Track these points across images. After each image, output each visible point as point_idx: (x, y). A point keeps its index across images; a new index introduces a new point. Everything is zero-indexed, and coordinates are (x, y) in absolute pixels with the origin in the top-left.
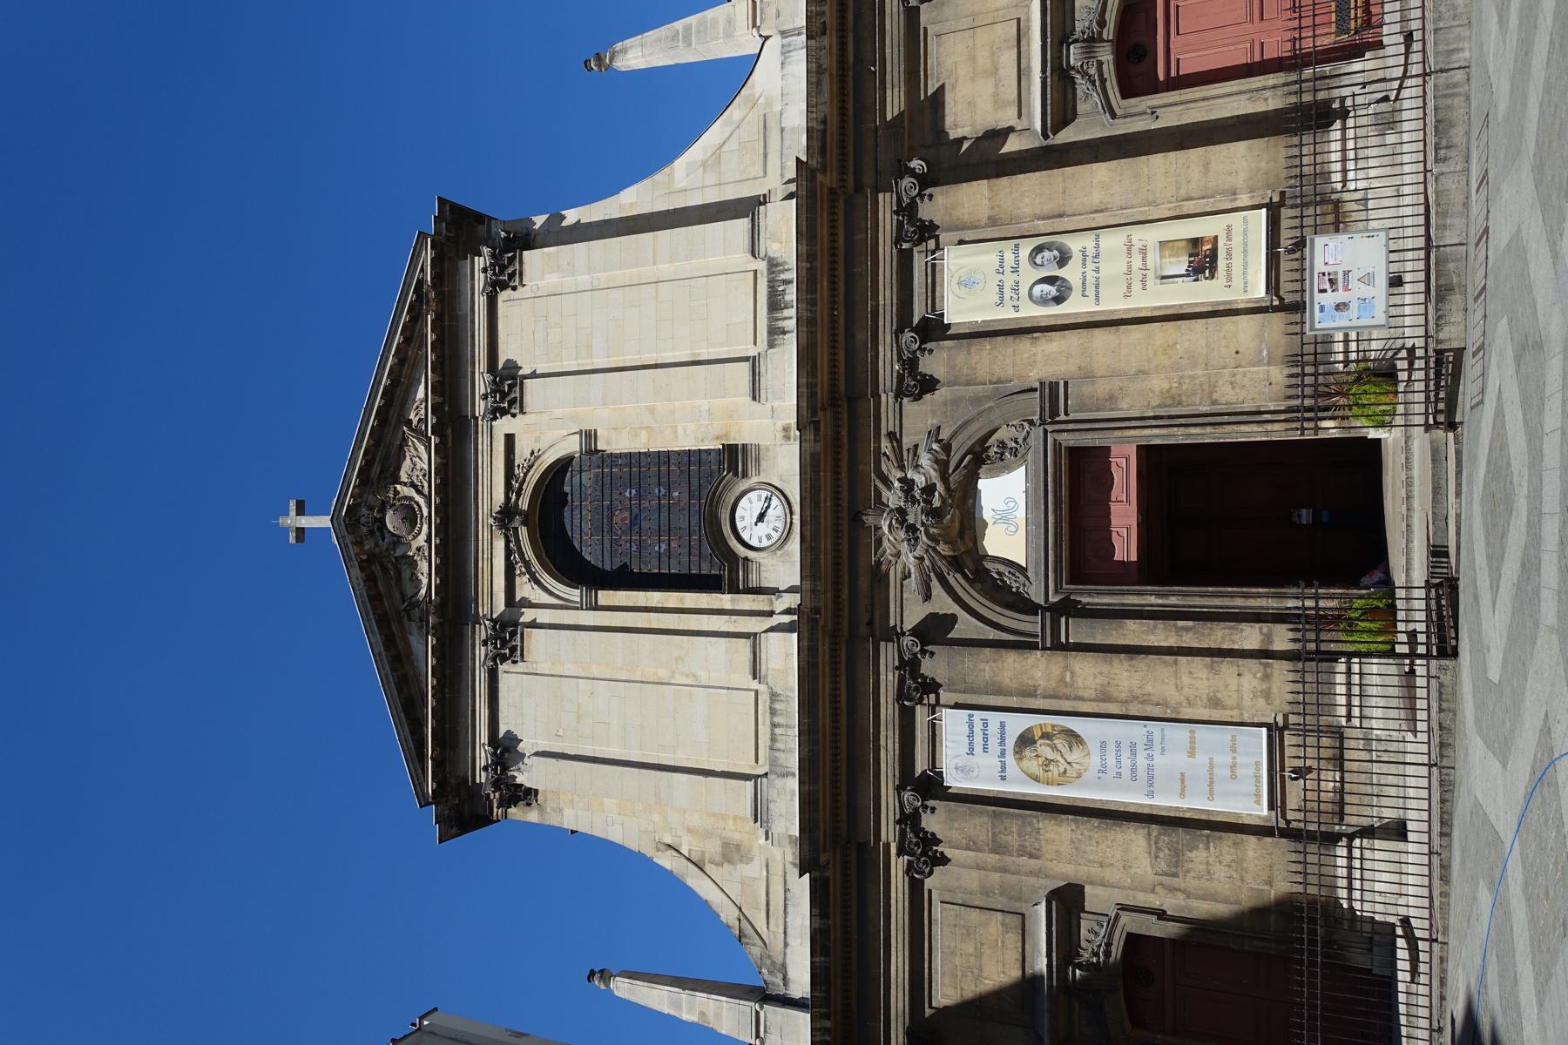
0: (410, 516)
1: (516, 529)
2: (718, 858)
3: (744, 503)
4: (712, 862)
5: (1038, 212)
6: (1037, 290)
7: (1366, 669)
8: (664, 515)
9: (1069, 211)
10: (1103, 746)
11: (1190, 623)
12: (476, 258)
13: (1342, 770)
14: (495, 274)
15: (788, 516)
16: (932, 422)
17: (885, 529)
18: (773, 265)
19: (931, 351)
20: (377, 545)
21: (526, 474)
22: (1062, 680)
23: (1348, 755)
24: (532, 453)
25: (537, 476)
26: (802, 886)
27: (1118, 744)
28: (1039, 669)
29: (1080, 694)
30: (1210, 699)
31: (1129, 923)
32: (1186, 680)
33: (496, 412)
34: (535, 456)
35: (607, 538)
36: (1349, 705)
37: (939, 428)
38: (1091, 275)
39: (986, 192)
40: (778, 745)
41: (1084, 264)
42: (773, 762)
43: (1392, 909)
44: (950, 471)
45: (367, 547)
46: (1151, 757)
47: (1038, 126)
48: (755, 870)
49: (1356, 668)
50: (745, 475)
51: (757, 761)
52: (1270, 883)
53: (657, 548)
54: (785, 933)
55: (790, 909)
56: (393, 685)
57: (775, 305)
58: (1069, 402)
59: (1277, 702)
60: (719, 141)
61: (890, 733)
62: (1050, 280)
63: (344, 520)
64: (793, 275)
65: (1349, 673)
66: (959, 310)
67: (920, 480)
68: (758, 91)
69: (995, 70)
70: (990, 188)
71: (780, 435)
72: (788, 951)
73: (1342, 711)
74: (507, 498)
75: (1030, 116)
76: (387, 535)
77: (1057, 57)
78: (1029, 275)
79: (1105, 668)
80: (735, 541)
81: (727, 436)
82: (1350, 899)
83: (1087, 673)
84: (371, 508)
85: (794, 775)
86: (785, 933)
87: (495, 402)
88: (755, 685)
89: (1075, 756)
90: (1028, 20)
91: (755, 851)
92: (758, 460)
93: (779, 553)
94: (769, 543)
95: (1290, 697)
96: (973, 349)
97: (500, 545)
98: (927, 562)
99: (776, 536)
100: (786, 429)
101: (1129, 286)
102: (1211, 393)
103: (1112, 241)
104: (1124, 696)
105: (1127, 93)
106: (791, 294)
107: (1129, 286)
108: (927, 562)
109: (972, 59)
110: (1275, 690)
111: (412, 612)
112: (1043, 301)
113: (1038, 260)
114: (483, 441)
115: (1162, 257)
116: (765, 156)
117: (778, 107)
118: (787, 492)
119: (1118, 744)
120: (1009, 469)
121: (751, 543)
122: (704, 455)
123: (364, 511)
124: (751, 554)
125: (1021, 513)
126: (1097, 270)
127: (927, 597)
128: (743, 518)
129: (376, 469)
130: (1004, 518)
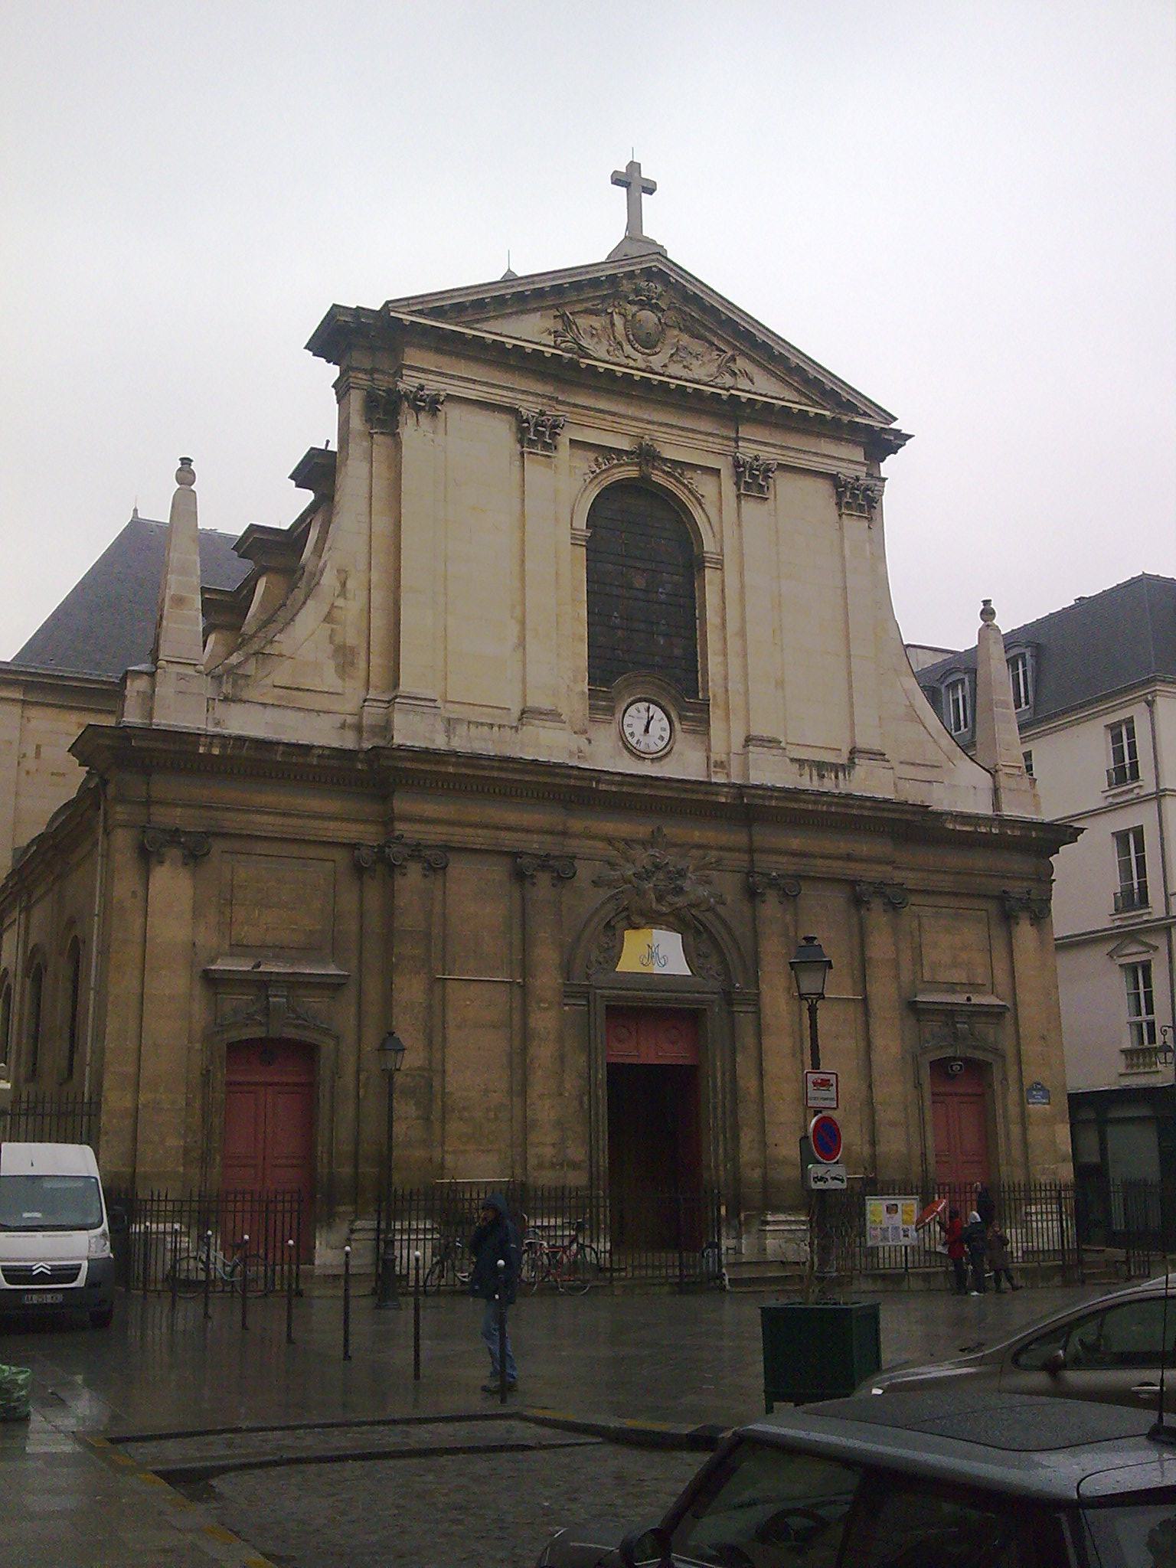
2: (338, 639)
3: (658, 714)
8: (642, 626)
9: (872, 1021)
14: (853, 488)
15: (651, 756)
16: (729, 899)
18: (848, 767)
31: (327, 1045)
37: (724, 904)
44: (693, 911)
48: (330, 679)
50: (681, 718)
51: (447, 702)
53: (615, 614)
56: (502, 292)
57: (821, 767)
58: (742, 1015)
63: (655, 266)
67: (687, 885)
75: (923, 991)
76: (635, 308)
80: (629, 701)
88: (516, 712)
92: (694, 732)
93: (620, 744)
94: (627, 735)
97: (625, 444)
99: (633, 741)
100: (721, 765)
106: (828, 785)
118: (667, 760)
124: (618, 715)
125: (657, 970)
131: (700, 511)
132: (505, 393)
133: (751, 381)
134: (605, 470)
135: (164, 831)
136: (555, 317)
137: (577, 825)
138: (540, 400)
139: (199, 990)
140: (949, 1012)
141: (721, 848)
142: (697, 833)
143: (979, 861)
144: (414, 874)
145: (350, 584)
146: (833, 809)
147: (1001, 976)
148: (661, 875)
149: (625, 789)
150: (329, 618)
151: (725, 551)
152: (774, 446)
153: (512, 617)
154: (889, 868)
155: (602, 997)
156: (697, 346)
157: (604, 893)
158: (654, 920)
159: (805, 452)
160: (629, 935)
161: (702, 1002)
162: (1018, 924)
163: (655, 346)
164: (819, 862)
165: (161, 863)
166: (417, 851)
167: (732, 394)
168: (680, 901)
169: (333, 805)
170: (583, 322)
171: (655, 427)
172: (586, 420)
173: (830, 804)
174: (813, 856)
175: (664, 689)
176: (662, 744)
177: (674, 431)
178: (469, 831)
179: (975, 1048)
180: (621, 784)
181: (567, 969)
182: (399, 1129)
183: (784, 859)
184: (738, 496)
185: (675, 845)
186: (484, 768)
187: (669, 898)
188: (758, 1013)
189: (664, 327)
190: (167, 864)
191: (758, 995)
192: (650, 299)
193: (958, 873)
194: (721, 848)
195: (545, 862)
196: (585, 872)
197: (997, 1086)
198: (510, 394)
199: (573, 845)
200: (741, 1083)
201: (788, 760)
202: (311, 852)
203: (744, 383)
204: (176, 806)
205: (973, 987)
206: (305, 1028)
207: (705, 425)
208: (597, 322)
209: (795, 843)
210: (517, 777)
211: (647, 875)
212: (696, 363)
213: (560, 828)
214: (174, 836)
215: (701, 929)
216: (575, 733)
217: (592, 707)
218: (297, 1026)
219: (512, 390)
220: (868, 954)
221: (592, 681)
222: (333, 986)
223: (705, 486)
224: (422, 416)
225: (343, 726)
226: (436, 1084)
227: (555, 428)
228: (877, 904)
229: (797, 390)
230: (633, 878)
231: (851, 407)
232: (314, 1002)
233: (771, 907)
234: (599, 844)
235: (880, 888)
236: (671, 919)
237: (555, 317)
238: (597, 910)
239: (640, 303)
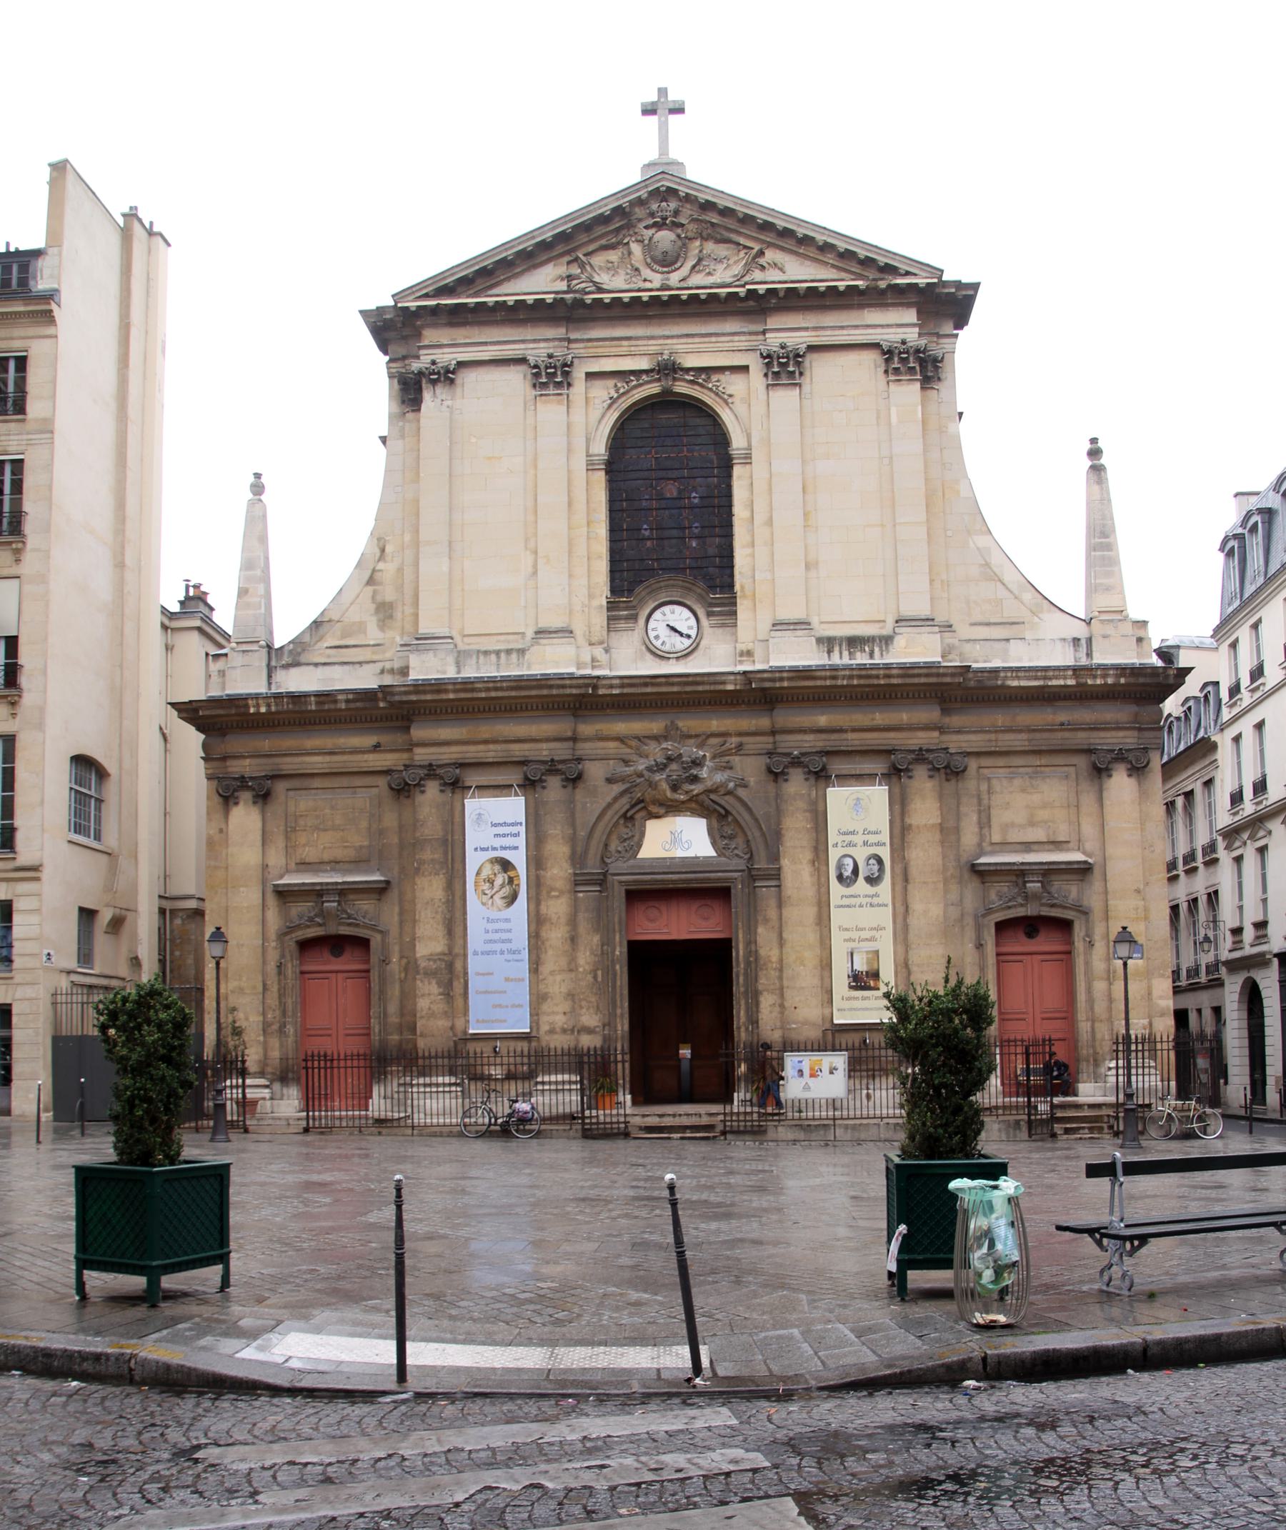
0: (667, 262)
1: (659, 380)
2: (379, 598)
3: (687, 613)
4: (375, 592)
5: (912, 863)
6: (849, 862)
7: (574, 1093)
9: (910, 887)
10: (507, 920)
11: (600, 979)
12: (917, 330)
13: (502, 1080)
14: (900, 353)
16: (752, 781)
17: (664, 745)
19: (807, 779)
20: (640, 220)
21: (710, 390)
22: (552, 889)
23: (513, 1083)
24: (730, 396)
25: (709, 401)
26: (366, 680)
27: (510, 931)
28: (559, 871)
29: (543, 903)
30: (546, 994)
31: (376, 940)
32: (559, 978)
33: (768, 358)
34: (726, 400)
35: (654, 475)
36: (550, 1083)
37: (745, 786)
38: (857, 901)
39: (931, 822)
40: (482, 657)
41: (866, 896)
42: (467, 654)
43: (416, 1110)
44: (713, 796)
45: (637, 210)
46: (502, 953)
47: (982, 860)
48: (374, 634)
49: (574, 1087)
50: (709, 614)
52: (421, 1035)
54: (325, 664)
55: (346, 668)
57: (854, 643)
59: (547, 1038)
60: (1006, 579)
61: (500, 754)
62: (856, 871)
64: (877, 660)
65: (570, 1082)
66: (838, 798)
67: (704, 773)
68: (1045, 616)
69: (1032, 823)
70: (933, 826)
71: (741, 647)
72: (311, 668)
73: (546, 1079)
74: (688, 370)
75: (992, 853)
76: (650, 232)
77: (1032, 872)
78: (861, 855)
79: (563, 920)
81: (744, 596)
82: (418, 1085)
83: (557, 908)
84: (676, 213)
85: (459, 672)
86: (325, 664)
87: (779, 358)
88: (530, 633)
89: (499, 901)
90: (1068, 850)
91: (390, 634)
92: (723, 626)
93: (644, 648)
95: (552, 1046)
96: (808, 814)
97: (644, 364)
98: (638, 780)
99: (658, 643)
100: (749, 653)
101: (847, 930)
102: (767, 990)
103: (885, 917)
104: (543, 934)
105: (1001, 927)
106: (861, 659)
107: (847, 930)
108: (638, 780)
109: (1044, 806)
110: (556, 1037)
111: (575, 265)
112: (840, 866)
113: (872, 861)
114: (741, 342)
115: (868, 952)
116: (988, 624)
117: (1028, 636)
118: (695, 654)
119: (510, 931)
120: (714, 844)
121: (651, 620)
122: (728, 572)
123: (673, 205)
125: (679, 853)
126: (861, 906)
127: (609, 781)
128: (673, 612)
129: (715, 219)
130: (675, 839)
131: (728, 410)
132: (516, 346)
133: (781, 270)
134: (623, 394)
135: (235, 779)
136: (569, 263)
137: (586, 729)
138: (551, 344)
139: (272, 901)
140: (1019, 874)
141: (740, 734)
142: (715, 723)
143: (1063, 715)
144: (432, 788)
145: (389, 549)
146: (855, 682)
147: (1089, 828)
148: (674, 766)
149: (626, 691)
150: (371, 581)
151: (754, 443)
152: (806, 329)
153: (526, 548)
154: (936, 734)
155: (620, 882)
156: (721, 250)
157: (617, 788)
158: (673, 808)
159: (842, 328)
160: (653, 827)
161: (726, 880)
162: (1110, 776)
163: (675, 262)
164: (850, 736)
165: (236, 804)
166: (431, 771)
167: (749, 290)
168: (697, 789)
169: (368, 740)
170: (598, 260)
171: (675, 341)
172: (592, 351)
173: (851, 677)
174: (845, 731)
175: (690, 589)
176: (687, 642)
177: (697, 340)
178: (482, 747)
179: (1053, 906)
180: (622, 686)
181: (577, 859)
182: (423, 1004)
183: (810, 737)
184: (768, 386)
185: (690, 737)
186: (480, 690)
187: (687, 787)
188: (779, 886)
189: (684, 242)
190: (242, 803)
191: (779, 869)
192: (665, 219)
193: (1034, 731)
194: (740, 734)
195: (552, 767)
196: (595, 772)
197: (1079, 945)
198: (522, 346)
199: (585, 748)
200: (762, 952)
201: (814, 640)
202: (358, 781)
203: (773, 275)
204: (244, 757)
205: (1056, 845)
206: (357, 925)
207: (731, 326)
208: (614, 256)
209: (823, 720)
210: (513, 693)
211: (661, 767)
212: (720, 267)
213: (569, 734)
214: (243, 782)
215: (723, 812)
216: (591, 644)
217: (609, 619)
218: (349, 925)
219: (523, 341)
220: (908, 821)
221: (615, 590)
222: (381, 890)
223: (734, 385)
224: (439, 389)
225: (382, 672)
226: (458, 965)
227: (566, 369)
228: (920, 772)
229: (833, 266)
230: (646, 773)
231: (889, 269)
232: (365, 905)
233: (796, 784)
234: (612, 744)
235: (920, 756)
236: (693, 805)
237: (569, 263)
238: (609, 806)
239: (655, 225)
